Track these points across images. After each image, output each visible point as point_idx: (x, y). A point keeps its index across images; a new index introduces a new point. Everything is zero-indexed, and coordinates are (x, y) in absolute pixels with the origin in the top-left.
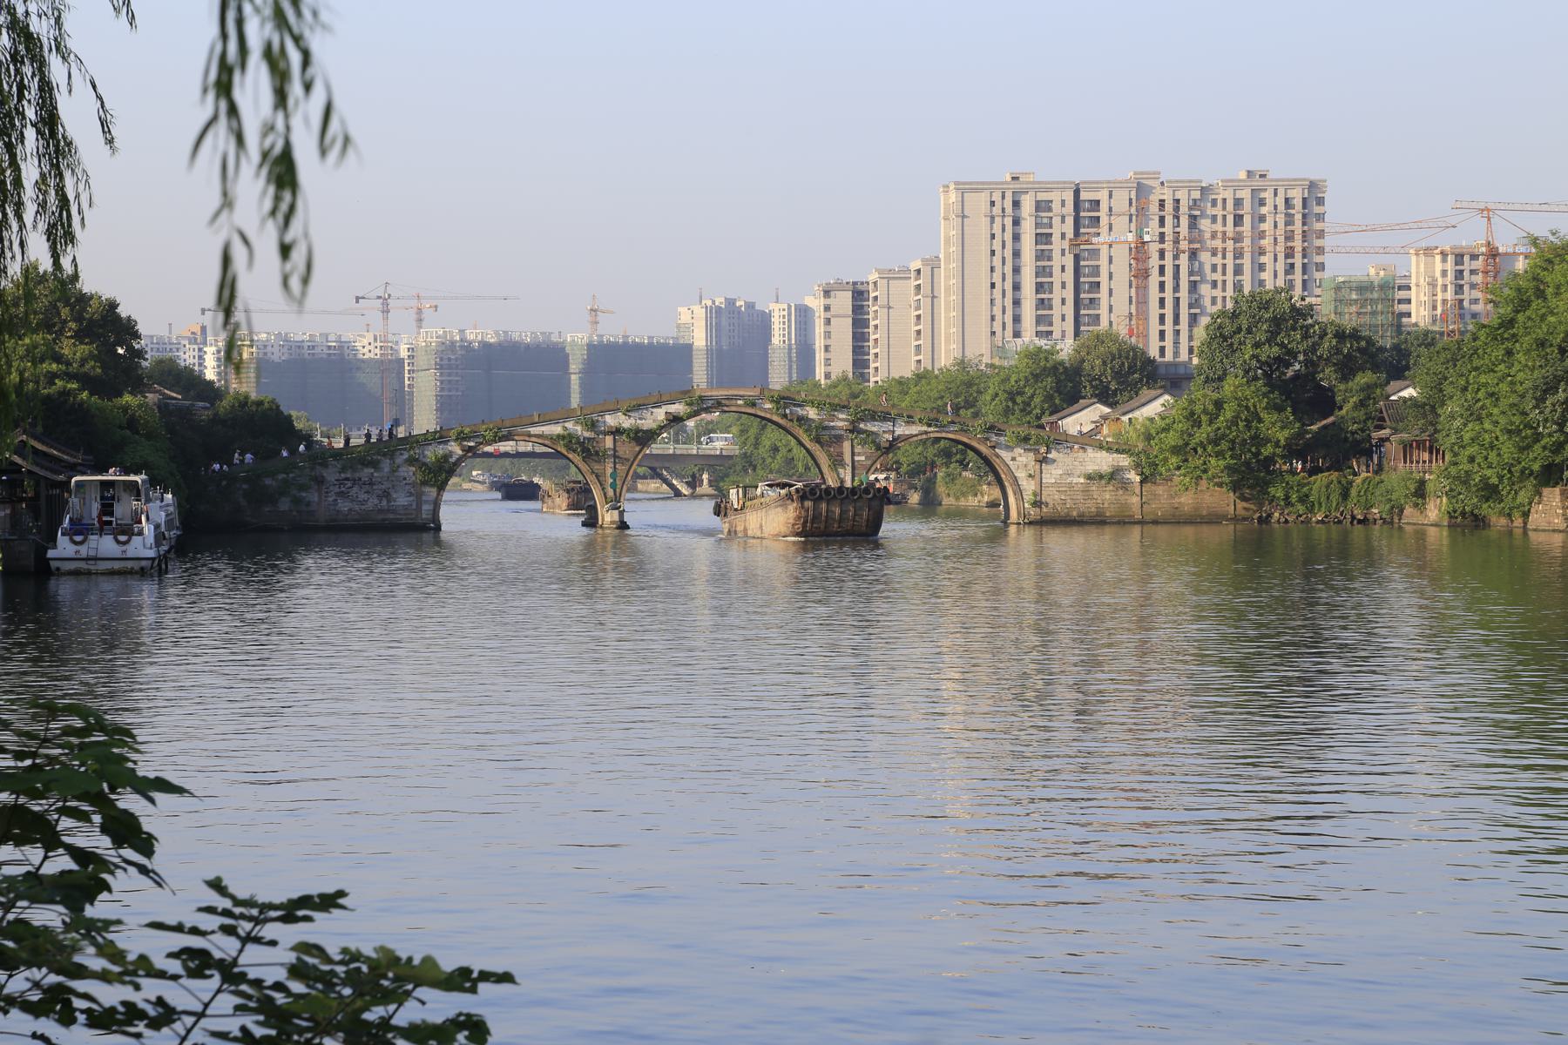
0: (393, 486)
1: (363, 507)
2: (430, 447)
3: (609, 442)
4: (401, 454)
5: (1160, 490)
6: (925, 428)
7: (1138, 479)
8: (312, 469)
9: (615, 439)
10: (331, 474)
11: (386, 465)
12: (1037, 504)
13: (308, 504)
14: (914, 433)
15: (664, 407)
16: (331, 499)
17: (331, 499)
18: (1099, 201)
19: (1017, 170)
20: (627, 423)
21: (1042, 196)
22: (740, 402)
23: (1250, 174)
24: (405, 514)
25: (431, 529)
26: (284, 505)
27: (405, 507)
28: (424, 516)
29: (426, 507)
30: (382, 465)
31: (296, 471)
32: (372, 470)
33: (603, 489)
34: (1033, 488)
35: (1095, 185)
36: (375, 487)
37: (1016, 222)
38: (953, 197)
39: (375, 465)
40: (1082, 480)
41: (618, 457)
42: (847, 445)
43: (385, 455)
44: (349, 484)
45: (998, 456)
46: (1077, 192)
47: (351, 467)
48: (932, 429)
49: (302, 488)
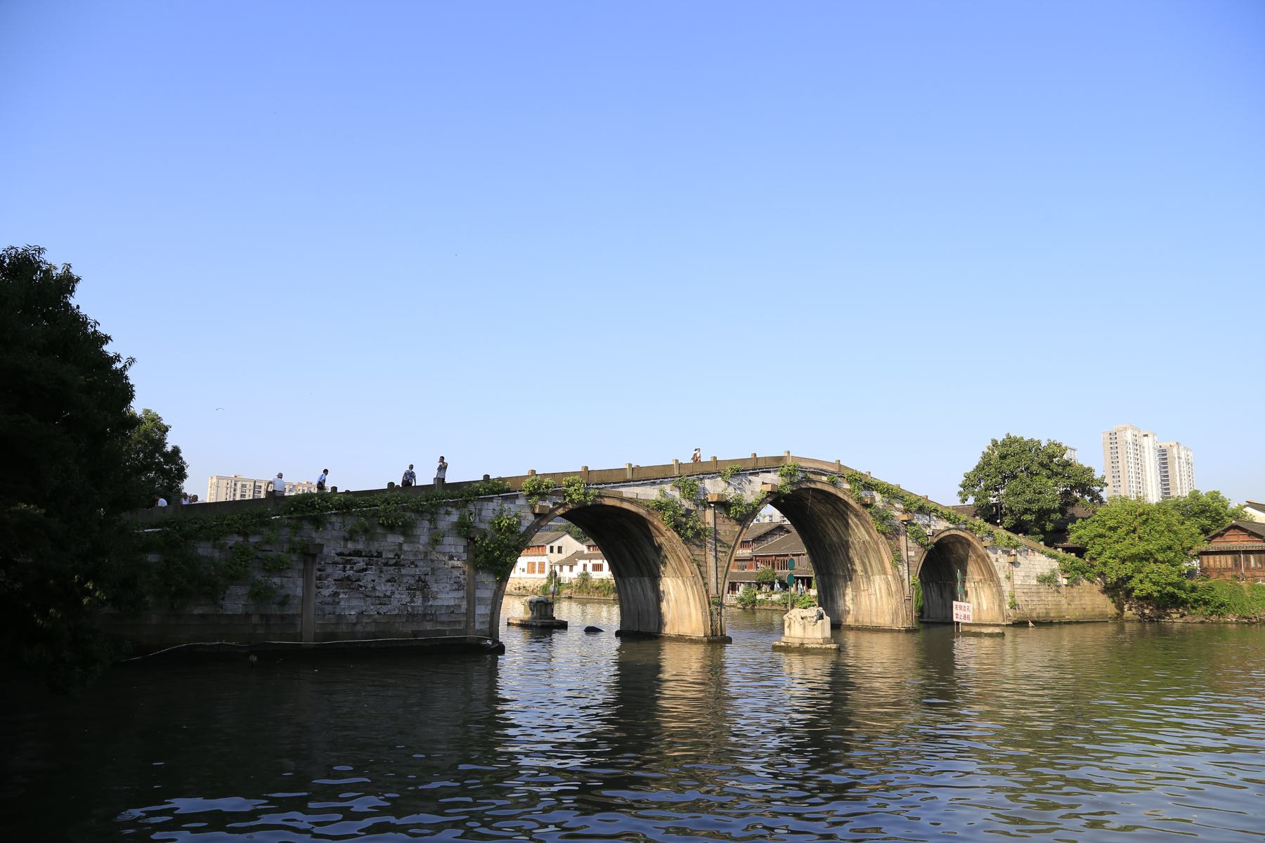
0: (433, 569)
1: (383, 609)
2: (491, 505)
3: (709, 515)
4: (448, 513)
5: (1075, 590)
6: (947, 524)
7: (1065, 582)
8: (296, 529)
9: (715, 513)
10: (331, 541)
11: (423, 531)
12: (1014, 606)
13: (285, 601)
14: (942, 528)
15: (761, 475)
16: (326, 592)
17: (326, 592)
18: (261, 486)
19: (236, 474)
20: (731, 493)
21: (244, 483)
22: (824, 479)
23: (307, 482)
24: (449, 623)
25: (483, 650)
26: (236, 602)
27: (451, 610)
28: (478, 626)
29: (482, 610)
30: (418, 532)
31: (266, 531)
32: (401, 539)
33: (705, 584)
34: (1009, 589)
35: (261, 481)
36: (403, 571)
37: (235, 490)
38: (215, 480)
39: (407, 530)
40: (1035, 582)
41: (720, 541)
42: (902, 538)
43: (419, 511)
44: (361, 563)
45: (989, 557)
46: (255, 482)
47: (366, 531)
48: (951, 526)
49: (277, 567)
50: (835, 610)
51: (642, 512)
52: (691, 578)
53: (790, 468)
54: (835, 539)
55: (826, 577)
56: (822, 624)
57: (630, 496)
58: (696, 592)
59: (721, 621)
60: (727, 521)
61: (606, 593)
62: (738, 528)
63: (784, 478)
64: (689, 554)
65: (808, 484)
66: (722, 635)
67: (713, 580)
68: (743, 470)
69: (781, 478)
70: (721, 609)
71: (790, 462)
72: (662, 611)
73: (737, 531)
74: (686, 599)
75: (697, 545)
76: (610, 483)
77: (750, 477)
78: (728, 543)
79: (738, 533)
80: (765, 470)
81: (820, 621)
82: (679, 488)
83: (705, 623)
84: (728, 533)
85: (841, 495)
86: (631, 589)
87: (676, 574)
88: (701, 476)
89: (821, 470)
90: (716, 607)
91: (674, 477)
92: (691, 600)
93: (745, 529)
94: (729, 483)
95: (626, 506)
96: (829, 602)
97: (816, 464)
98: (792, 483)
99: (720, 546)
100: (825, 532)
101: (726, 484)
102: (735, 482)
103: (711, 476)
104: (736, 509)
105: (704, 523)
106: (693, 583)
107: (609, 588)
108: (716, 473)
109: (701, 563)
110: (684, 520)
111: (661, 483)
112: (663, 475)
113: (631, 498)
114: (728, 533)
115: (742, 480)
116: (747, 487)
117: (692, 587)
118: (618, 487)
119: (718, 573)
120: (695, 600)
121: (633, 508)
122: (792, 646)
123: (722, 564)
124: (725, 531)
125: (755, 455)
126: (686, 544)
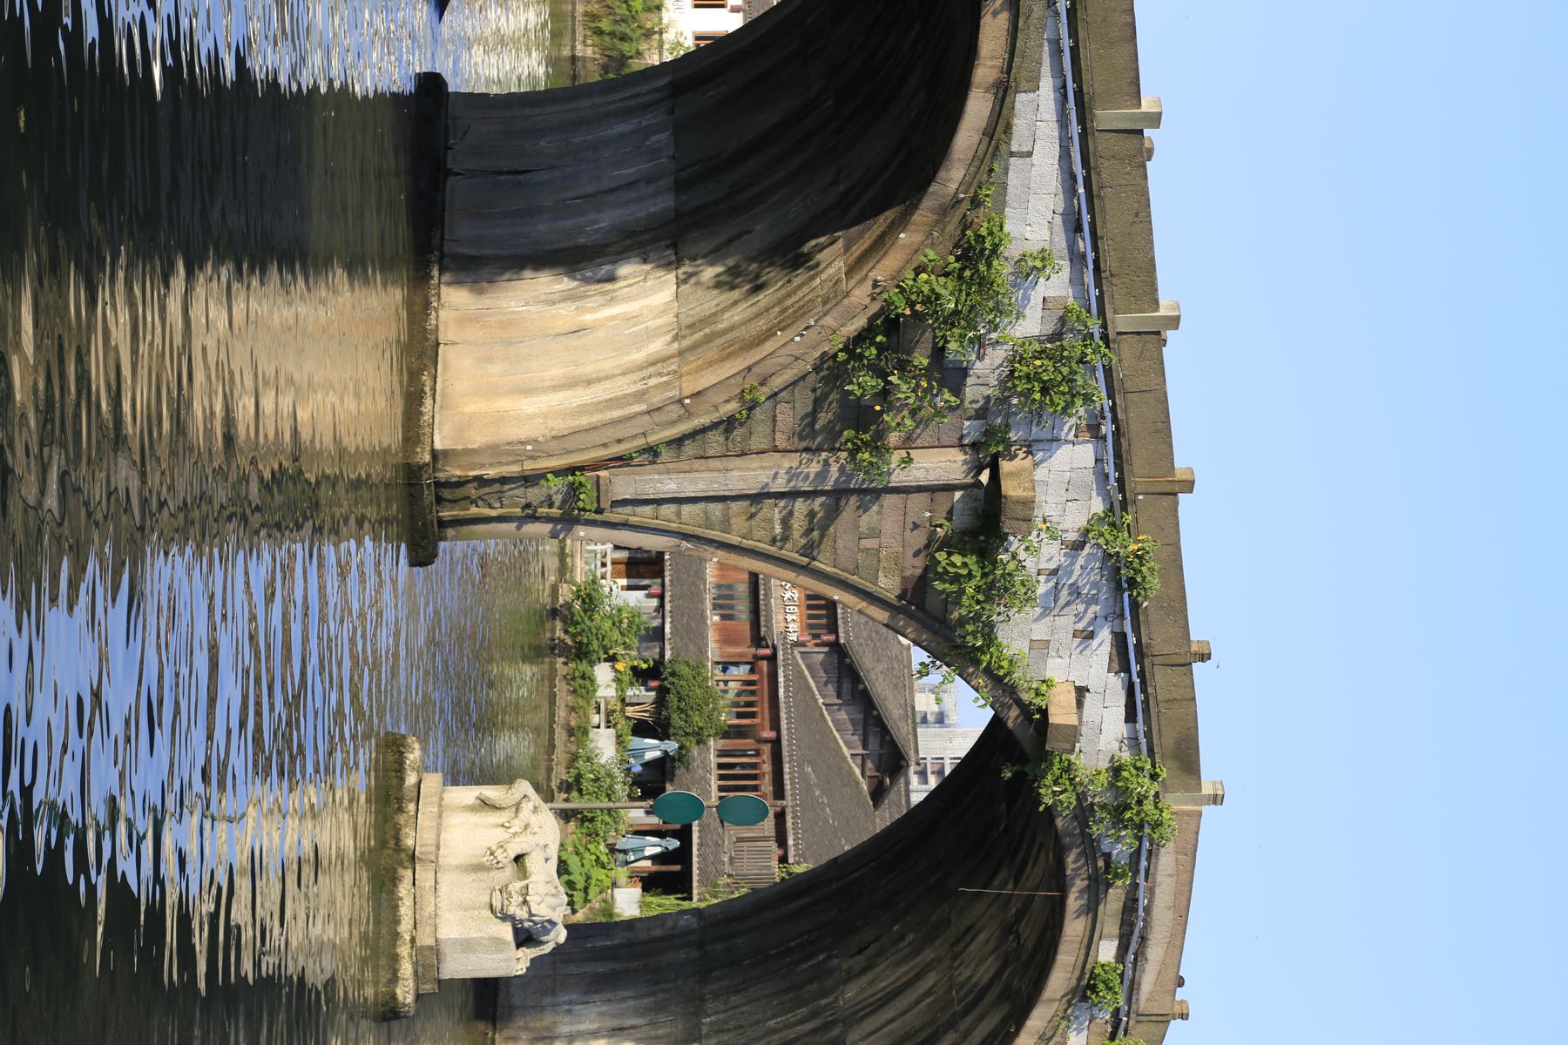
9: (949, 488)
15: (1116, 683)
22: (1107, 951)
33: (652, 452)
41: (833, 512)
50: (554, 993)
51: (953, 177)
52: (674, 393)
53: (1148, 806)
54: (851, 992)
55: (695, 954)
56: (497, 942)
57: (1020, 124)
58: (616, 414)
59: (501, 519)
60: (919, 539)
61: (605, 25)
62: (888, 585)
63: (1104, 779)
64: (778, 382)
65: (1080, 884)
66: (443, 524)
67: (670, 485)
68: (1135, 606)
69: (1104, 765)
70: (549, 519)
71: (1176, 803)
72: (528, 273)
73: (875, 583)
74: (587, 369)
75: (813, 416)
76: (1073, 33)
77: (1105, 636)
78: (827, 544)
79: (870, 587)
80: (1139, 697)
81: (506, 931)
82: (1056, 336)
83: (495, 451)
84: (865, 543)
85: (1037, 1020)
86: (622, 135)
87: (691, 326)
88: (1107, 428)
89: (1143, 939)
90: (558, 499)
91: (1102, 313)
92: (582, 396)
93: (882, 615)
94: (1078, 546)
95: (978, 107)
96: (589, 968)
97: (1170, 915)
98: (1084, 812)
99: (811, 515)
100: (880, 953)
101: (1072, 536)
102: (1085, 571)
103: (1110, 468)
104: (970, 576)
105: (908, 442)
106: (656, 399)
107: (623, 38)
108: (1122, 489)
109: (738, 433)
110: (921, 359)
111: (1076, 258)
112: (1110, 262)
113: (1008, 128)
114: (865, 543)
115: (1094, 600)
116: (1066, 623)
117: (640, 396)
118: (1058, 72)
119: (702, 505)
120: (583, 410)
121: (967, 136)
122: (402, 819)
123: (738, 523)
124: (875, 533)
125: (1204, 657)
126: (817, 369)
